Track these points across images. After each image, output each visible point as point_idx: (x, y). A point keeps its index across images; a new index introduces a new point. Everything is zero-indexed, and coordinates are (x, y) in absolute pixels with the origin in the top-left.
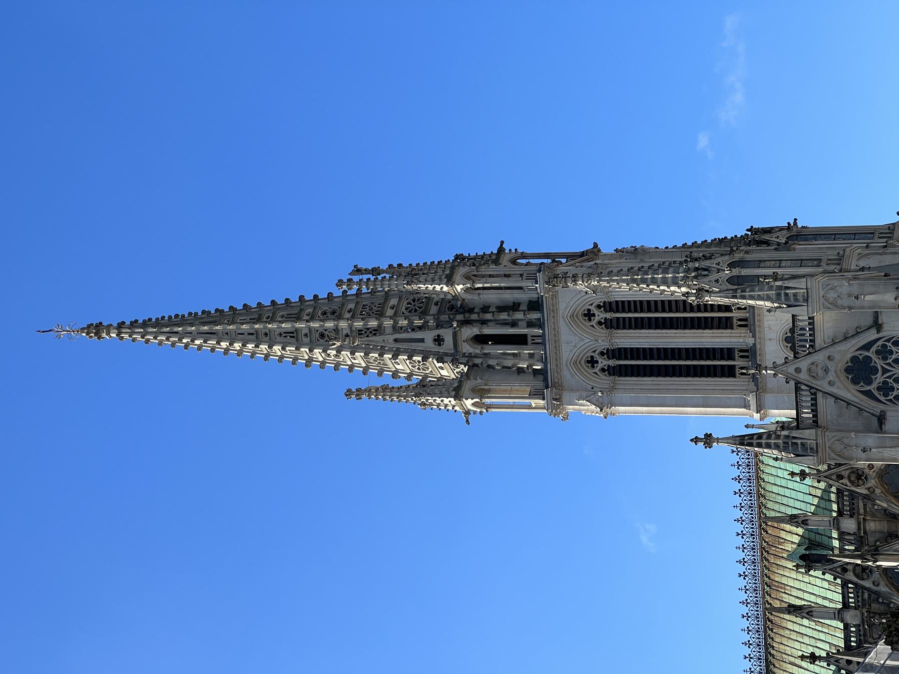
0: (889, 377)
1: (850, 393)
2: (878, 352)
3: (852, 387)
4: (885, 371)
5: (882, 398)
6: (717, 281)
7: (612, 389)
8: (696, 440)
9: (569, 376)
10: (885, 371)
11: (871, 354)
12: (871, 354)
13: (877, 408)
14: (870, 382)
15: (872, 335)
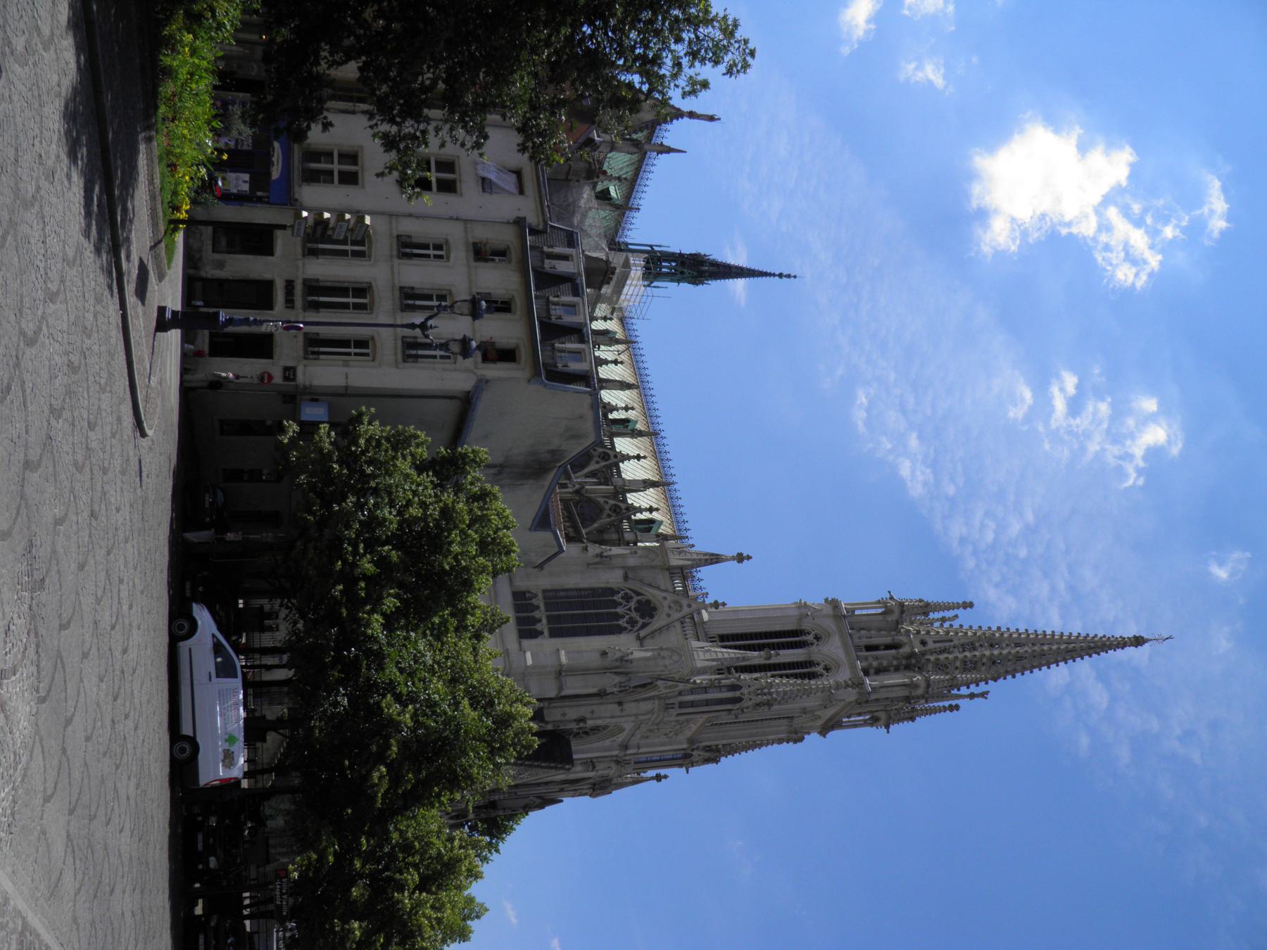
0: (625, 606)
1: (650, 593)
2: (637, 622)
3: (650, 597)
4: (630, 609)
5: (628, 591)
6: (749, 686)
7: (801, 618)
8: (749, 558)
9: (830, 625)
10: (630, 609)
11: (641, 621)
12: (641, 621)
13: (630, 584)
14: (639, 602)
15: (642, 633)
